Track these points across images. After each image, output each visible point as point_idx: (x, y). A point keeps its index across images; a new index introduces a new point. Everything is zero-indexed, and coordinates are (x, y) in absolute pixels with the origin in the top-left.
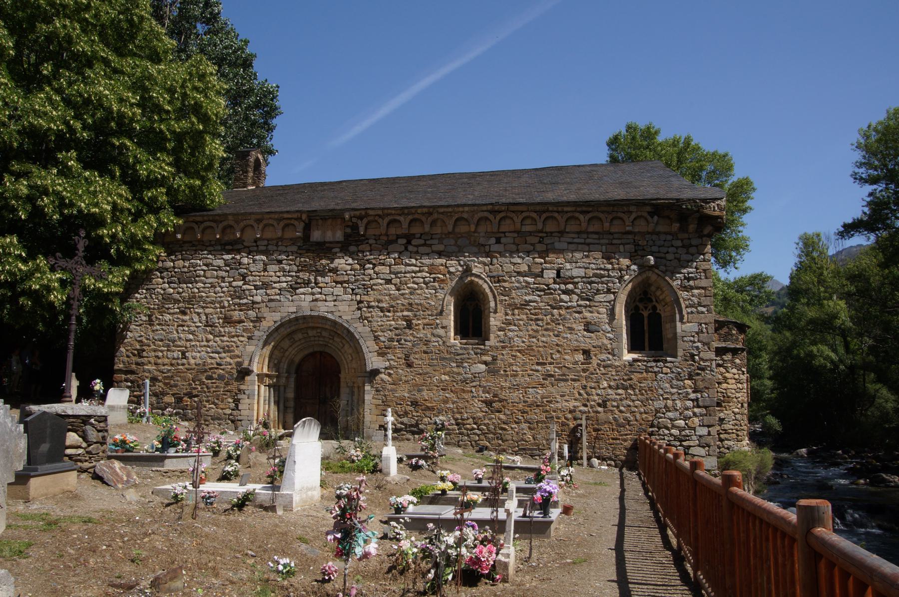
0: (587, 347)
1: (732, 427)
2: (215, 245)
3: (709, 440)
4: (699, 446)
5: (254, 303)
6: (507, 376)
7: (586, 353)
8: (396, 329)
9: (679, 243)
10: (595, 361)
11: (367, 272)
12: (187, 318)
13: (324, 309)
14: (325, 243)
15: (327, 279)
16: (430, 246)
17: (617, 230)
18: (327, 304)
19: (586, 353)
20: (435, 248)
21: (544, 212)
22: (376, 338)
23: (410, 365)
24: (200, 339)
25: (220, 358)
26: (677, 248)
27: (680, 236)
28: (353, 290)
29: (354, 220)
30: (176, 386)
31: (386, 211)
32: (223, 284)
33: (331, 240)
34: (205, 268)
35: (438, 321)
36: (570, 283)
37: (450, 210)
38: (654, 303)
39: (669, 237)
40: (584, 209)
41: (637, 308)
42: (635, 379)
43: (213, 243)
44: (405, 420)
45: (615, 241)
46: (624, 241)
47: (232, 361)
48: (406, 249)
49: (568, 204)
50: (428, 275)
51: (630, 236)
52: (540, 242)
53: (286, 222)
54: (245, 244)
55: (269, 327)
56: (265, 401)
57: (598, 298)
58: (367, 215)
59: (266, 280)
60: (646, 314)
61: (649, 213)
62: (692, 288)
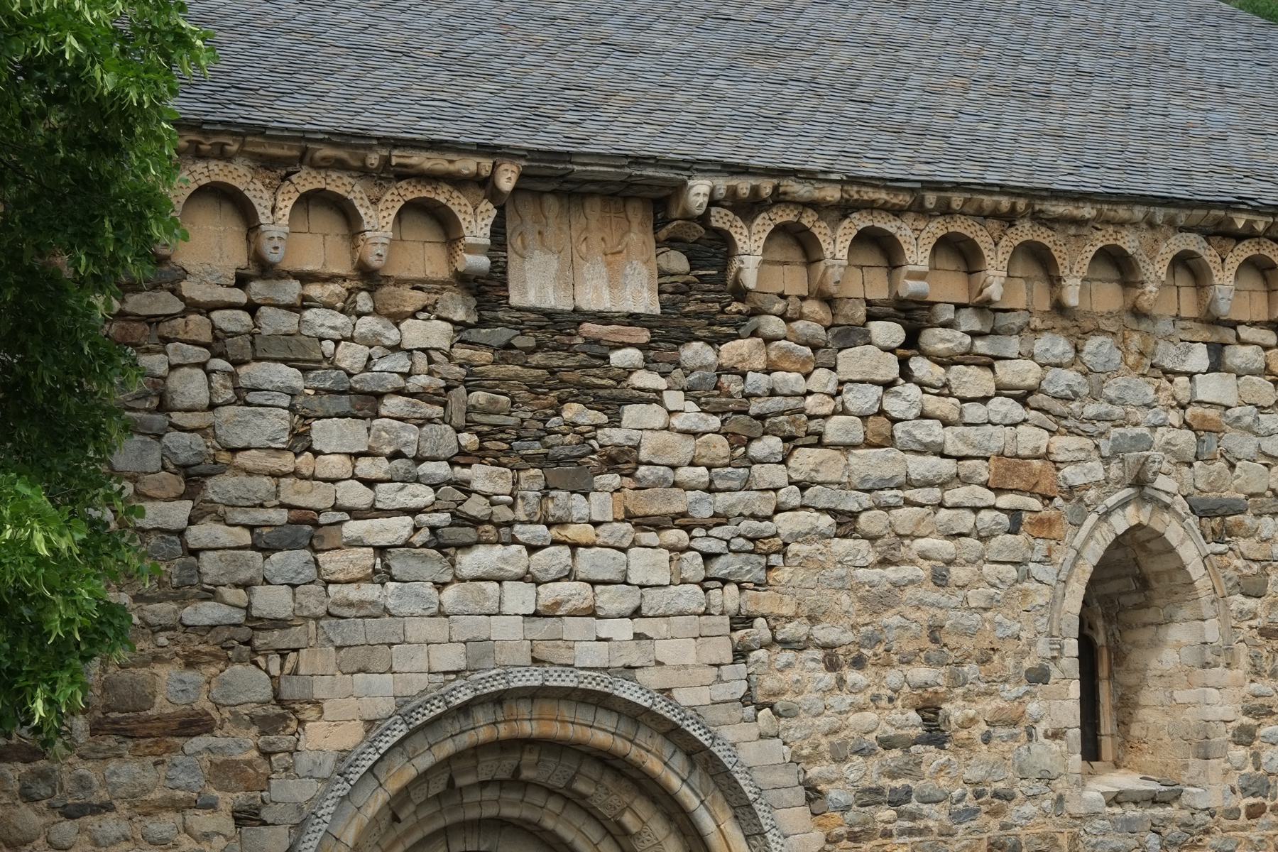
5: (258, 624)
8: (887, 743)
13: (588, 651)
14: (579, 316)
15: (599, 504)
18: (605, 628)
20: (1009, 372)
22: (813, 794)
28: (708, 557)
29: (721, 218)
35: (1033, 707)
37: (1087, 211)
48: (906, 374)
50: (990, 497)
53: (413, 192)
54: (191, 289)
58: (779, 198)
59: (314, 497)
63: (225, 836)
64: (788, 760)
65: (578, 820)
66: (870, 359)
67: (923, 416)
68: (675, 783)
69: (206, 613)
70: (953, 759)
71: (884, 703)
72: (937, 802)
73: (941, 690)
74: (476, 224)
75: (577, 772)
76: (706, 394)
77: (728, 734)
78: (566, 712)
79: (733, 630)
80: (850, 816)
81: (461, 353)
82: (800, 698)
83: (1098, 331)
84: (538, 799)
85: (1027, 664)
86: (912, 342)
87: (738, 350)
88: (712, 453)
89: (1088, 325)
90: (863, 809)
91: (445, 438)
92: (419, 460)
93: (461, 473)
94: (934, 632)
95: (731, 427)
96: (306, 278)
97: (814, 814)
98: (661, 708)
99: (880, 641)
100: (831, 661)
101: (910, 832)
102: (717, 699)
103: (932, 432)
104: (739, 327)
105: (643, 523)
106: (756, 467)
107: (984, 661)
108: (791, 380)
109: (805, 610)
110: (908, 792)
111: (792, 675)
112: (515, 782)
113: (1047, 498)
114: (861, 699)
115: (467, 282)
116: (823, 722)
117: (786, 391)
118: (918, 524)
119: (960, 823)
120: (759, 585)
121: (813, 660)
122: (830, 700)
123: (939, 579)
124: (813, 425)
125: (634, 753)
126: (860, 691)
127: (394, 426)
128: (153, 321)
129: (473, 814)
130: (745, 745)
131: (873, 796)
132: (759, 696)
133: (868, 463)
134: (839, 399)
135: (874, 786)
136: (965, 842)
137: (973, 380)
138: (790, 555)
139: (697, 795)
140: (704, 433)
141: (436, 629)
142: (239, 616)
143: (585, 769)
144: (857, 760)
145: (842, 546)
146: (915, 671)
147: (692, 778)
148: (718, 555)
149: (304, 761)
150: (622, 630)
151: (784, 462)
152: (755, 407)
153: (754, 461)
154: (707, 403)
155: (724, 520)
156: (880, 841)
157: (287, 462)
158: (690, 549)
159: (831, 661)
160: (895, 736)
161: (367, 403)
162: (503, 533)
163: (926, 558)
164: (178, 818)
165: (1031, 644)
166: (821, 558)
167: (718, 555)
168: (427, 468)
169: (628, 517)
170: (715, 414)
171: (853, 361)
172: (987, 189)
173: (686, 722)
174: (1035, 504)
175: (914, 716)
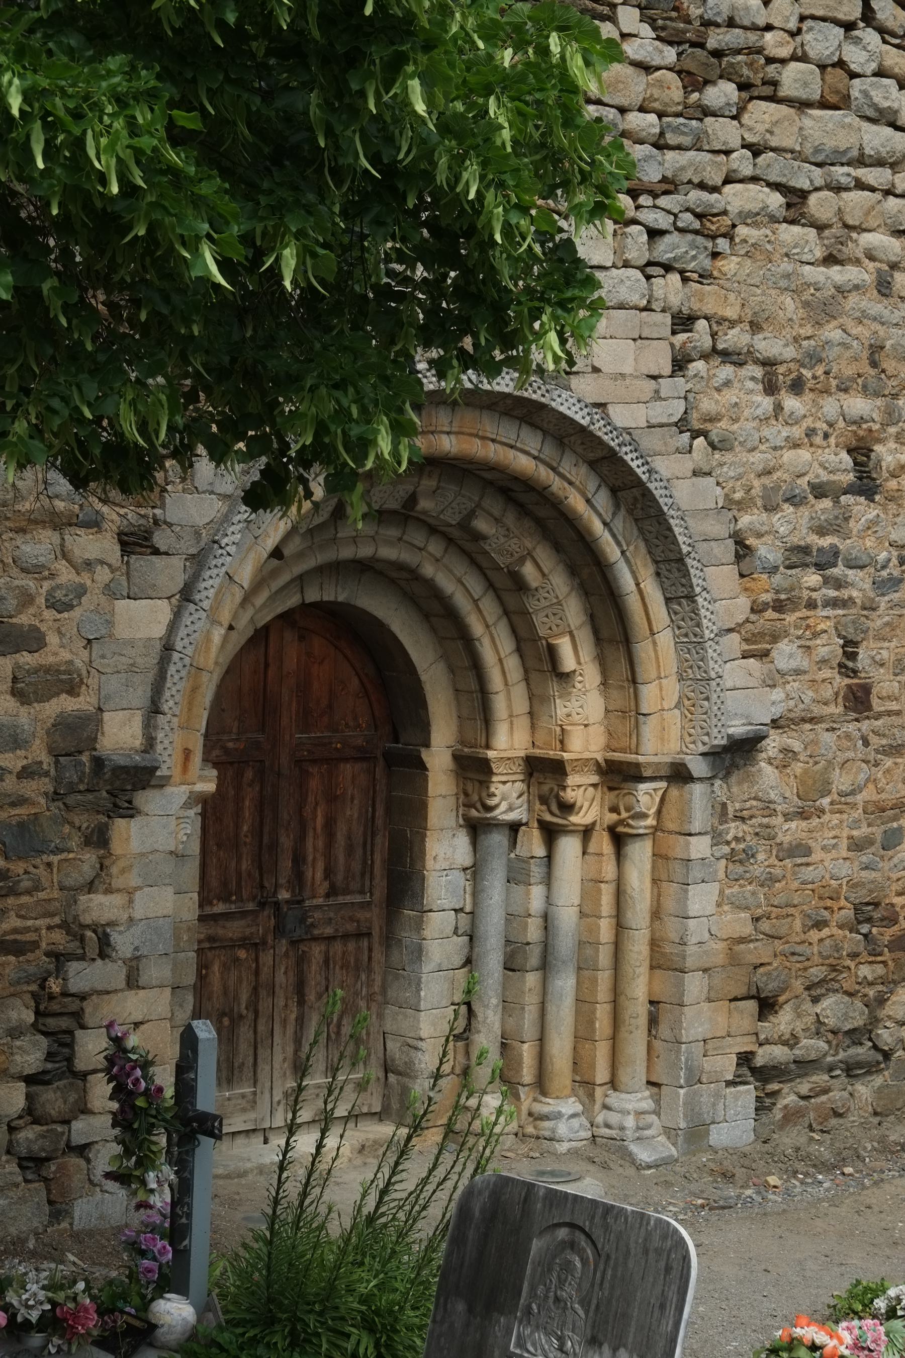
8: (819, 491)
22: (742, 550)
23: (859, 700)
47: (24, 716)
63: (110, 566)
64: (720, 506)
65: (460, 568)
67: (880, 73)
68: (597, 526)
70: (882, 515)
71: (818, 440)
72: (862, 567)
73: (876, 427)
75: (478, 506)
77: (659, 463)
78: (489, 425)
79: (674, 333)
80: (777, 579)
82: (736, 426)
88: (665, 95)
90: (789, 572)
95: (689, 65)
97: (742, 576)
98: (598, 429)
99: (820, 360)
100: (770, 381)
101: (834, 603)
102: (653, 421)
103: (887, 94)
106: (709, 120)
109: (749, 317)
110: (835, 552)
111: (730, 396)
114: (797, 432)
116: (757, 459)
117: (746, 23)
118: (867, 213)
119: (883, 595)
120: (704, 276)
121: (753, 379)
122: (766, 432)
124: (771, 69)
125: (557, 485)
126: (796, 423)
129: (346, 553)
130: (682, 486)
131: (801, 555)
133: (827, 129)
134: (798, 39)
135: (802, 543)
136: (887, 619)
138: (737, 240)
139: (618, 543)
140: (658, 68)
143: (487, 503)
144: (788, 509)
145: (790, 233)
146: (851, 400)
147: (616, 521)
148: (662, 233)
153: (707, 112)
154: (663, 28)
155: (672, 187)
156: (804, 613)
158: (635, 222)
159: (770, 381)
160: (829, 483)
163: (872, 258)
164: (56, 538)
166: (769, 247)
167: (662, 233)
170: (671, 43)
173: (624, 449)
175: (844, 455)
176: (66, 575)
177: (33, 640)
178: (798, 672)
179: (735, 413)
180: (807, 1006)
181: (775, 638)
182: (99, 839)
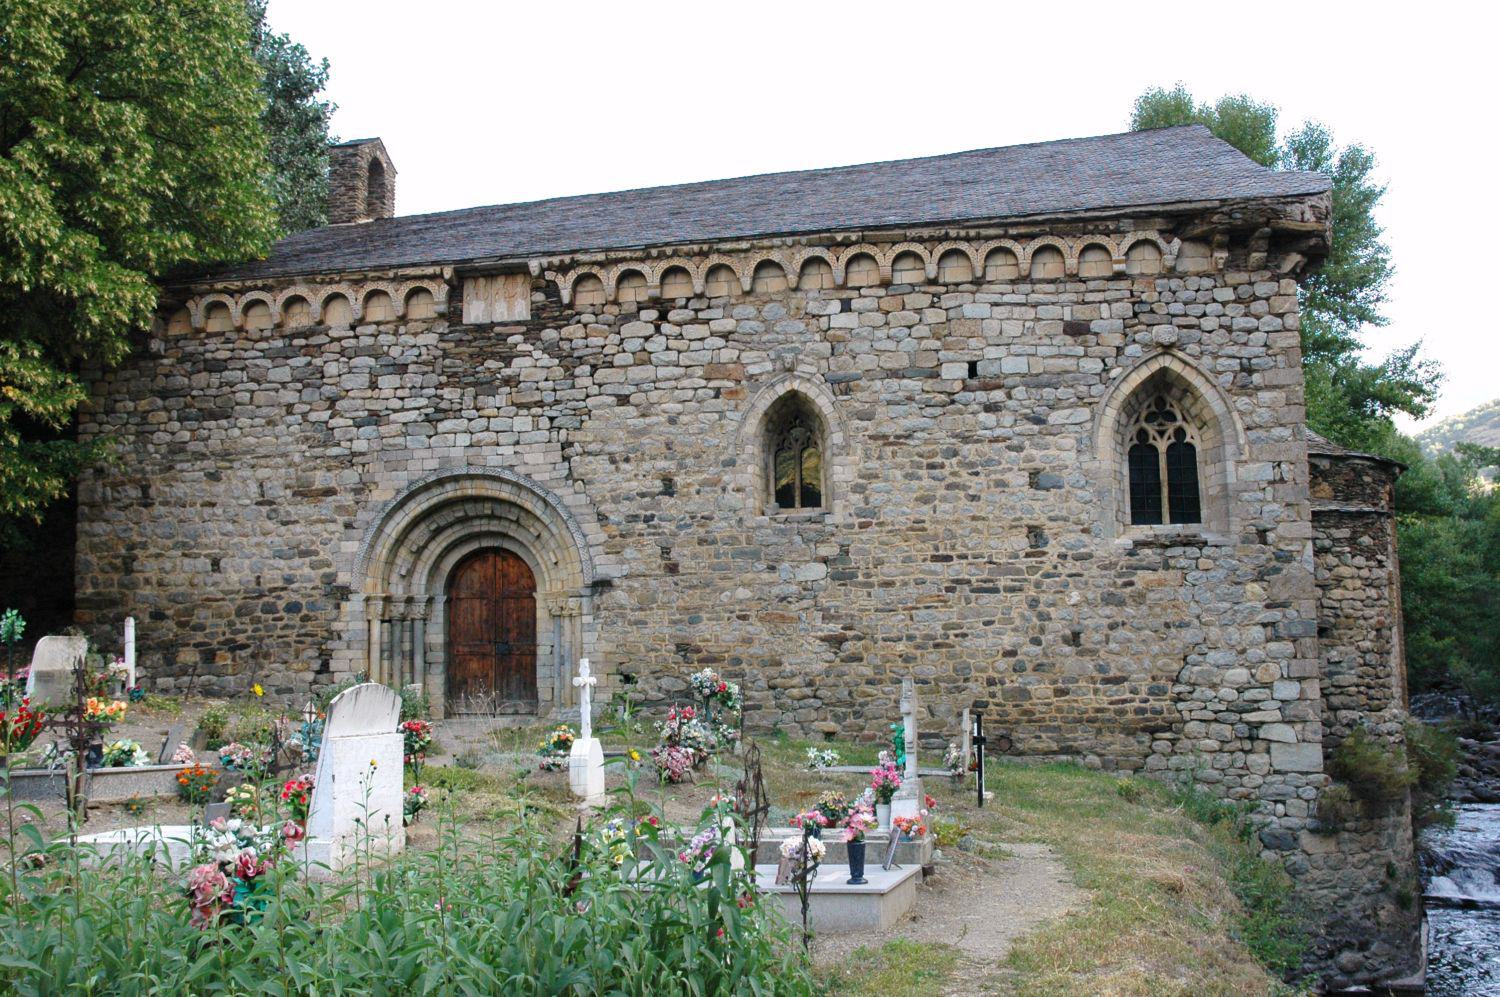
0: (1040, 518)
1: (1356, 680)
2: (272, 337)
3: (1304, 709)
4: (1283, 722)
5: (354, 454)
6: (871, 585)
7: (1035, 533)
8: (643, 495)
9: (1228, 294)
10: (1053, 549)
11: (579, 382)
12: (220, 488)
13: (492, 459)
14: (493, 325)
15: (501, 399)
16: (707, 322)
17: (1094, 274)
18: (500, 450)
19: (1035, 533)
20: (715, 326)
21: (940, 240)
22: (602, 518)
23: (673, 569)
24: (248, 530)
25: (290, 568)
26: (1224, 304)
27: (1233, 277)
28: (552, 419)
29: (549, 275)
30: (202, 628)
31: (613, 255)
32: (290, 419)
33: (506, 318)
34: (253, 386)
36: (999, 387)
37: (744, 245)
38: (1180, 422)
39: (1207, 283)
40: (1023, 230)
41: (1142, 434)
42: (1139, 585)
43: (267, 333)
44: (665, 683)
45: (1090, 297)
46: (1109, 295)
48: (658, 329)
49: (989, 222)
50: (703, 383)
51: (1124, 284)
52: (932, 305)
53: (412, 285)
54: (332, 333)
55: (385, 504)
56: (382, 651)
57: (1055, 417)
58: (574, 264)
60: (1162, 445)
61: (1161, 232)
62: (1258, 389)
66: (642, 326)
69: (335, 451)
74: (440, 291)
76: (551, 349)
78: (487, 484)
81: (442, 345)
83: (772, 300)
84: (507, 524)
85: (722, 458)
86: (663, 317)
87: (573, 330)
89: (765, 298)
91: (434, 379)
92: (422, 388)
93: (439, 392)
94: (668, 446)
96: (378, 324)
103: (673, 356)
104: (568, 320)
105: (520, 406)
107: (697, 457)
108: (600, 341)
110: (653, 516)
112: (492, 517)
113: (738, 382)
115: (442, 316)
116: (608, 486)
123: (672, 421)
127: (413, 378)
128: (320, 346)
129: (477, 529)
132: (575, 475)
133: (637, 373)
137: (692, 331)
141: (427, 453)
142: (347, 452)
145: (618, 410)
149: (370, 505)
150: (509, 451)
151: (592, 375)
152: (576, 354)
157: (369, 393)
161: (401, 369)
162: (457, 413)
165: (725, 448)
168: (425, 391)
169: (513, 404)
171: (627, 330)
172: (682, 243)
174: (731, 384)
176: (325, 535)
177: (316, 553)
178: (635, 559)
179: (595, 472)
180: (651, 680)
181: (623, 547)
182: (338, 607)
